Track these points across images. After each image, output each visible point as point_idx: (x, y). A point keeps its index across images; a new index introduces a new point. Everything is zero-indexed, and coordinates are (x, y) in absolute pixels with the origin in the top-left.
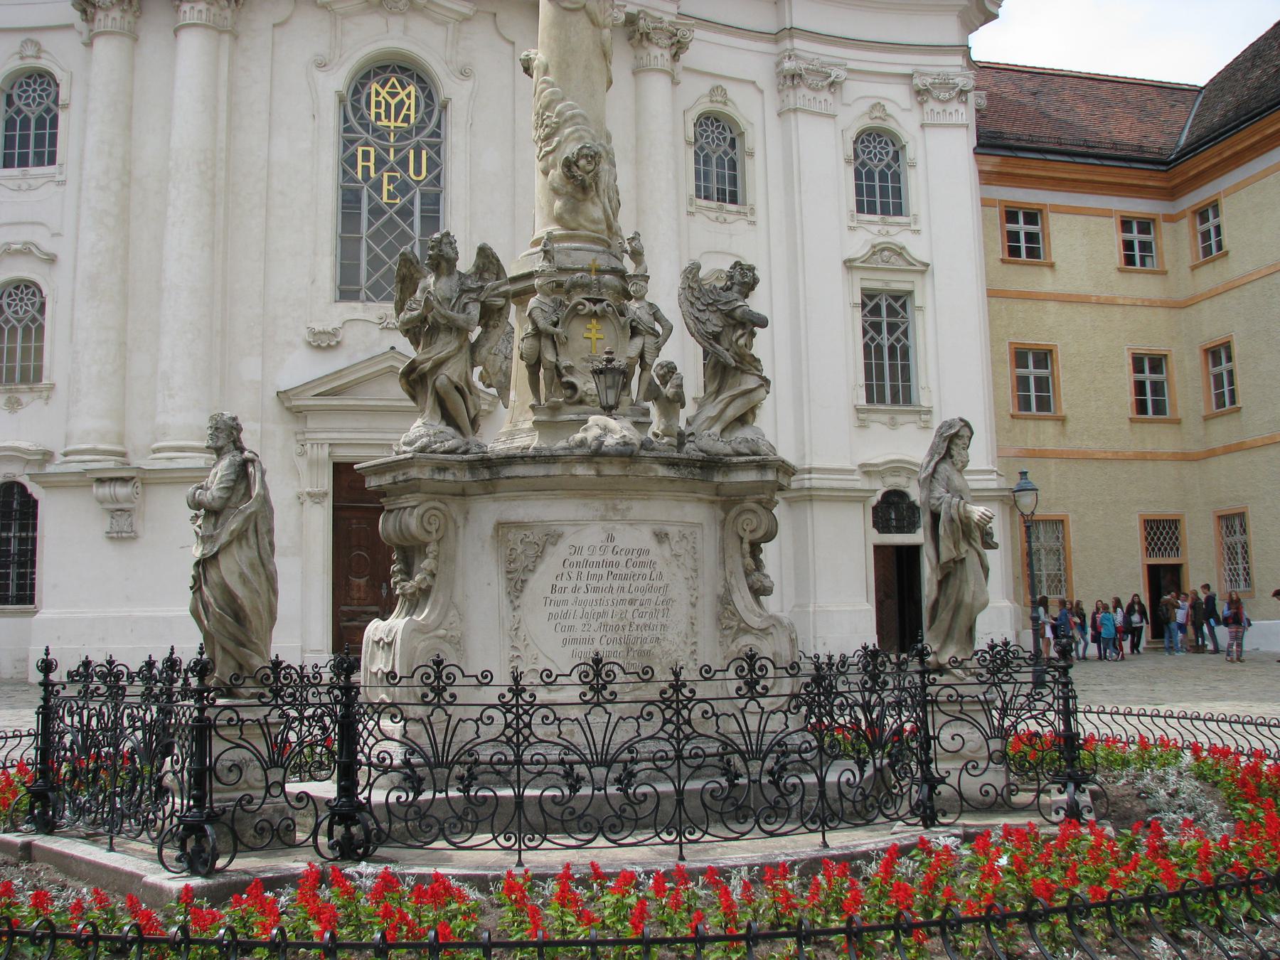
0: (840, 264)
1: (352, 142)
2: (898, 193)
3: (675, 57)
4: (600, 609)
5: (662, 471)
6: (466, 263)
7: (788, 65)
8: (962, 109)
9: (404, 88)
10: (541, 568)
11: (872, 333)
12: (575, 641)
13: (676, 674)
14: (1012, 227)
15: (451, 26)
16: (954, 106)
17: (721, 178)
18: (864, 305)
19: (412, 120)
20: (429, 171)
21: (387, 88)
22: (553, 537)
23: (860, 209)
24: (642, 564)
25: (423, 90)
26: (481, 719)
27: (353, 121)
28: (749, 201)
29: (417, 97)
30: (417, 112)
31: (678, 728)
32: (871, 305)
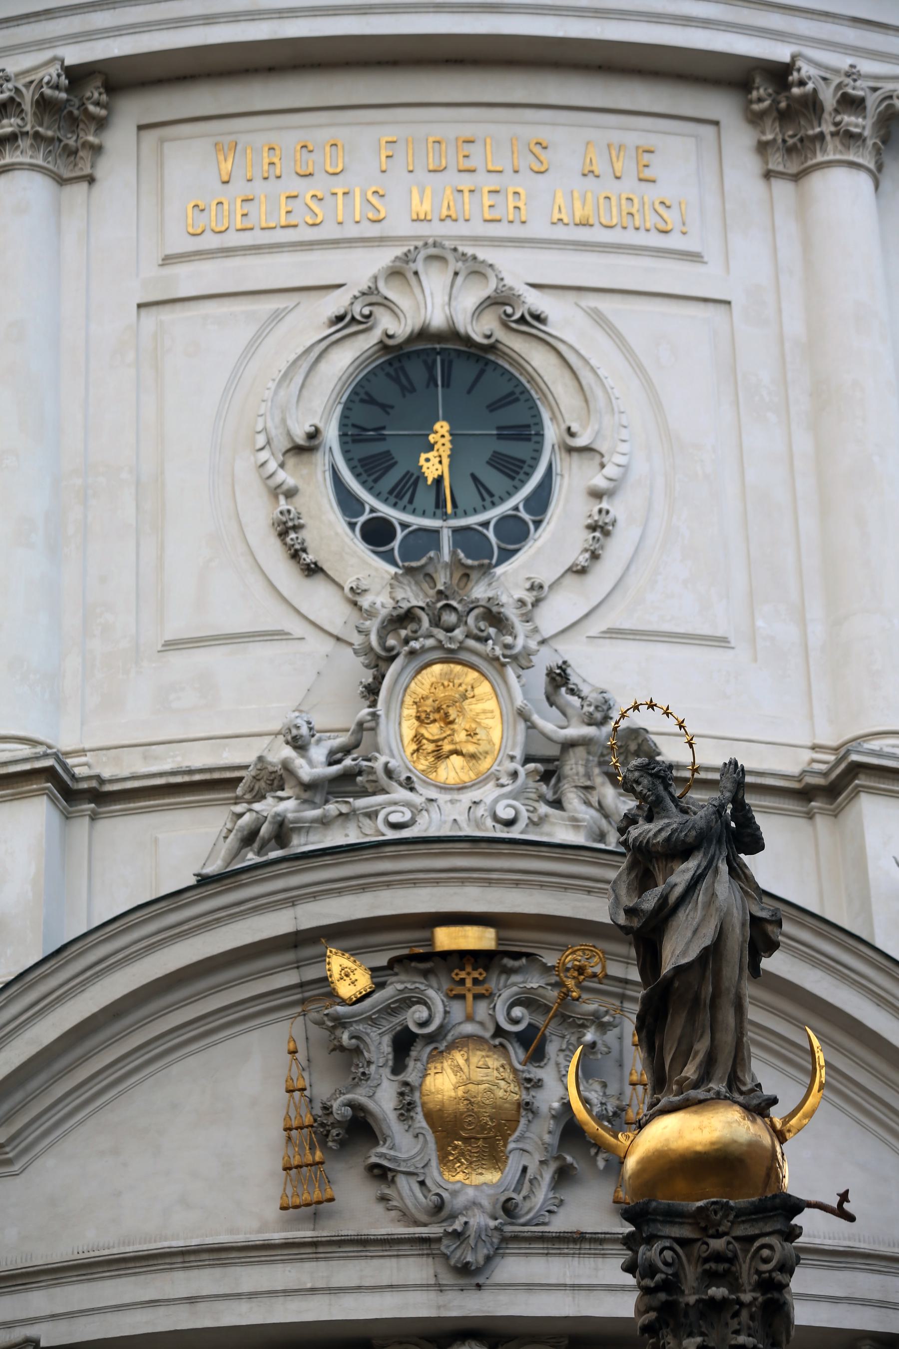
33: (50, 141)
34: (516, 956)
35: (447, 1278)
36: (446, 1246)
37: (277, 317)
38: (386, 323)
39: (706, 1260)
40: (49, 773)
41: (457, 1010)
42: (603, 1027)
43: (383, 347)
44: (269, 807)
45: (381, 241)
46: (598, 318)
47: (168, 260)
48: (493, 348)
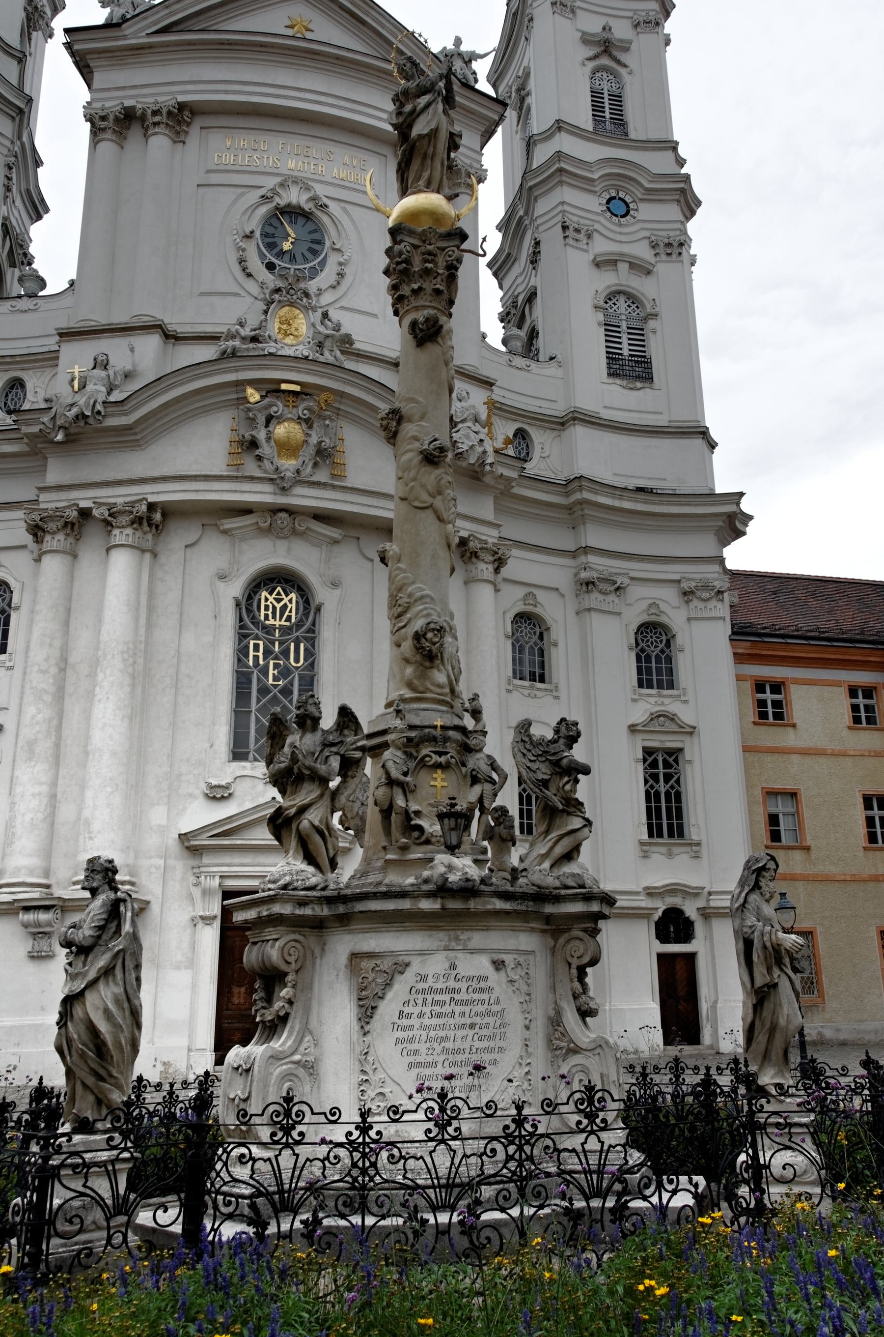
0: (625, 729)
1: (245, 636)
2: (670, 672)
3: (497, 571)
4: (442, 1034)
5: (499, 904)
6: (328, 721)
7: (584, 575)
8: (719, 605)
9: (287, 595)
10: (390, 995)
11: (651, 782)
12: (419, 1065)
13: (519, 1108)
14: (761, 696)
15: (324, 547)
16: (713, 603)
17: (532, 663)
18: (645, 760)
19: (293, 620)
20: (305, 660)
21: (274, 595)
22: (401, 967)
23: (641, 685)
24: (482, 990)
25: (302, 596)
26: (327, 1158)
27: (247, 620)
28: (554, 680)
29: (297, 602)
30: (297, 614)
31: (521, 1165)
32: (650, 759)
33: (171, 127)
34: (306, 394)
35: (277, 491)
36: (278, 481)
37: (243, 194)
38: (277, 200)
39: (424, 254)
40: (160, 327)
41: (286, 409)
42: (331, 420)
43: (277, 208)
44: (230, 343)
45: (278, 175)
46: (345, 210)
47: (208, 171)
48: (311, 213)
